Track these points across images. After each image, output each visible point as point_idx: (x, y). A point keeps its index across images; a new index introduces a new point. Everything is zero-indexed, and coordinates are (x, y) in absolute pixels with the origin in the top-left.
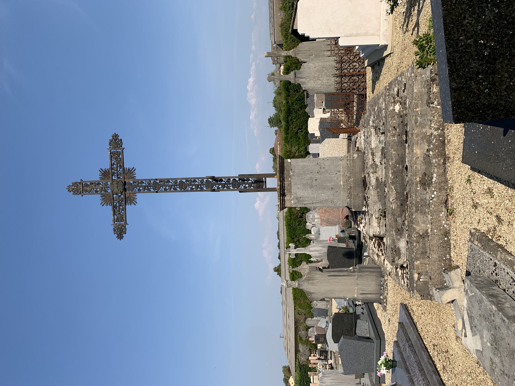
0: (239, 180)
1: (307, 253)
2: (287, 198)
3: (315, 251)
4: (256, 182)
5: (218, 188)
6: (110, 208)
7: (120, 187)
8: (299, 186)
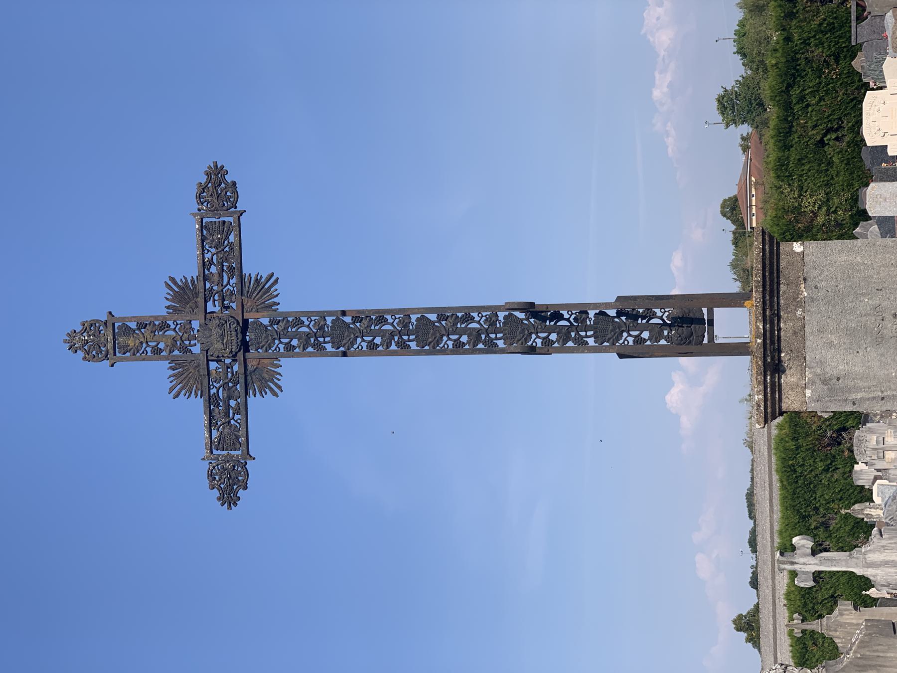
0: (619, 314)
1: (858, 571)
2: (788, 379)
3: (886, 563)
4: (678, 321)
5: (547, 342)
6: (198, 404)
7: (229, 337)
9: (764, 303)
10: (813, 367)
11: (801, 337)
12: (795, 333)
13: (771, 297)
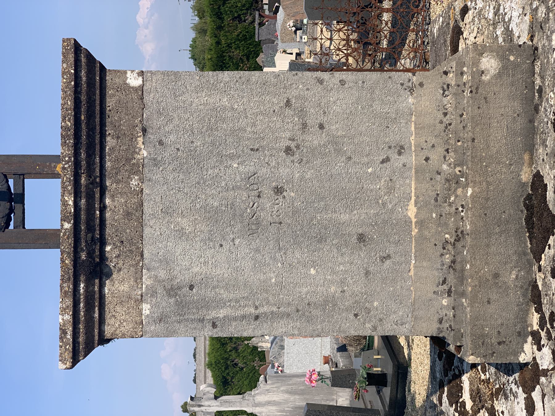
1: (249, 410)
2: (115, 288)
3: (269, 403)
8: (184, 222)
9: (77, 164)
10: (154, 268)
11: (137, 220)
12: (128, 214)
13: (90, 156)
